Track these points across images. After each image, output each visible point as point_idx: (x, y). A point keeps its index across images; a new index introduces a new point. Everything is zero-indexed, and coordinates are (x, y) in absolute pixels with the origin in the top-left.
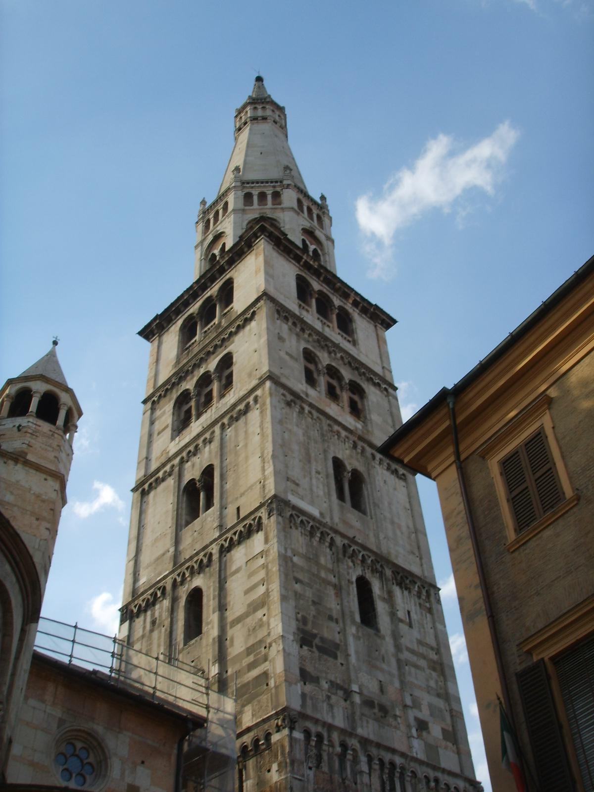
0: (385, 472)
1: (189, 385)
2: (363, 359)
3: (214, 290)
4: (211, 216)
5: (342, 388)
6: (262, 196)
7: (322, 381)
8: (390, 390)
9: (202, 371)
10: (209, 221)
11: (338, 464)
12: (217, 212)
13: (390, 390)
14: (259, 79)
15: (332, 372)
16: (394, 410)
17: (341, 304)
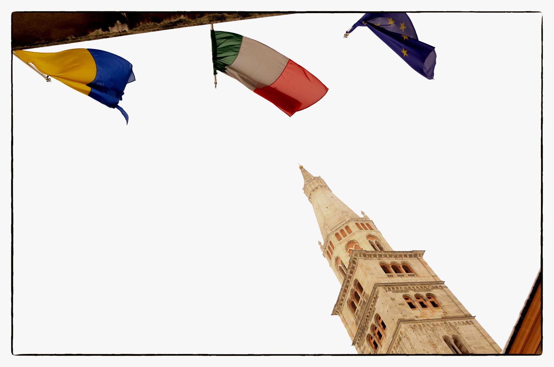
0: (463, 326)
1: (369, 331)
2: (424, 280)
3: (352, 286)
4: (328, 249)
5: (425, 300)
6: (342, 231)
7: (417, 304)
8: (442, 285)
9: (370, 324)
10: (328, 252)
11: (446, 340)
12: (329, 247)
13: (442, 285)
14: (301, 168)
15: (418, 297)
16: (449, 293)
17: (401, 261)
